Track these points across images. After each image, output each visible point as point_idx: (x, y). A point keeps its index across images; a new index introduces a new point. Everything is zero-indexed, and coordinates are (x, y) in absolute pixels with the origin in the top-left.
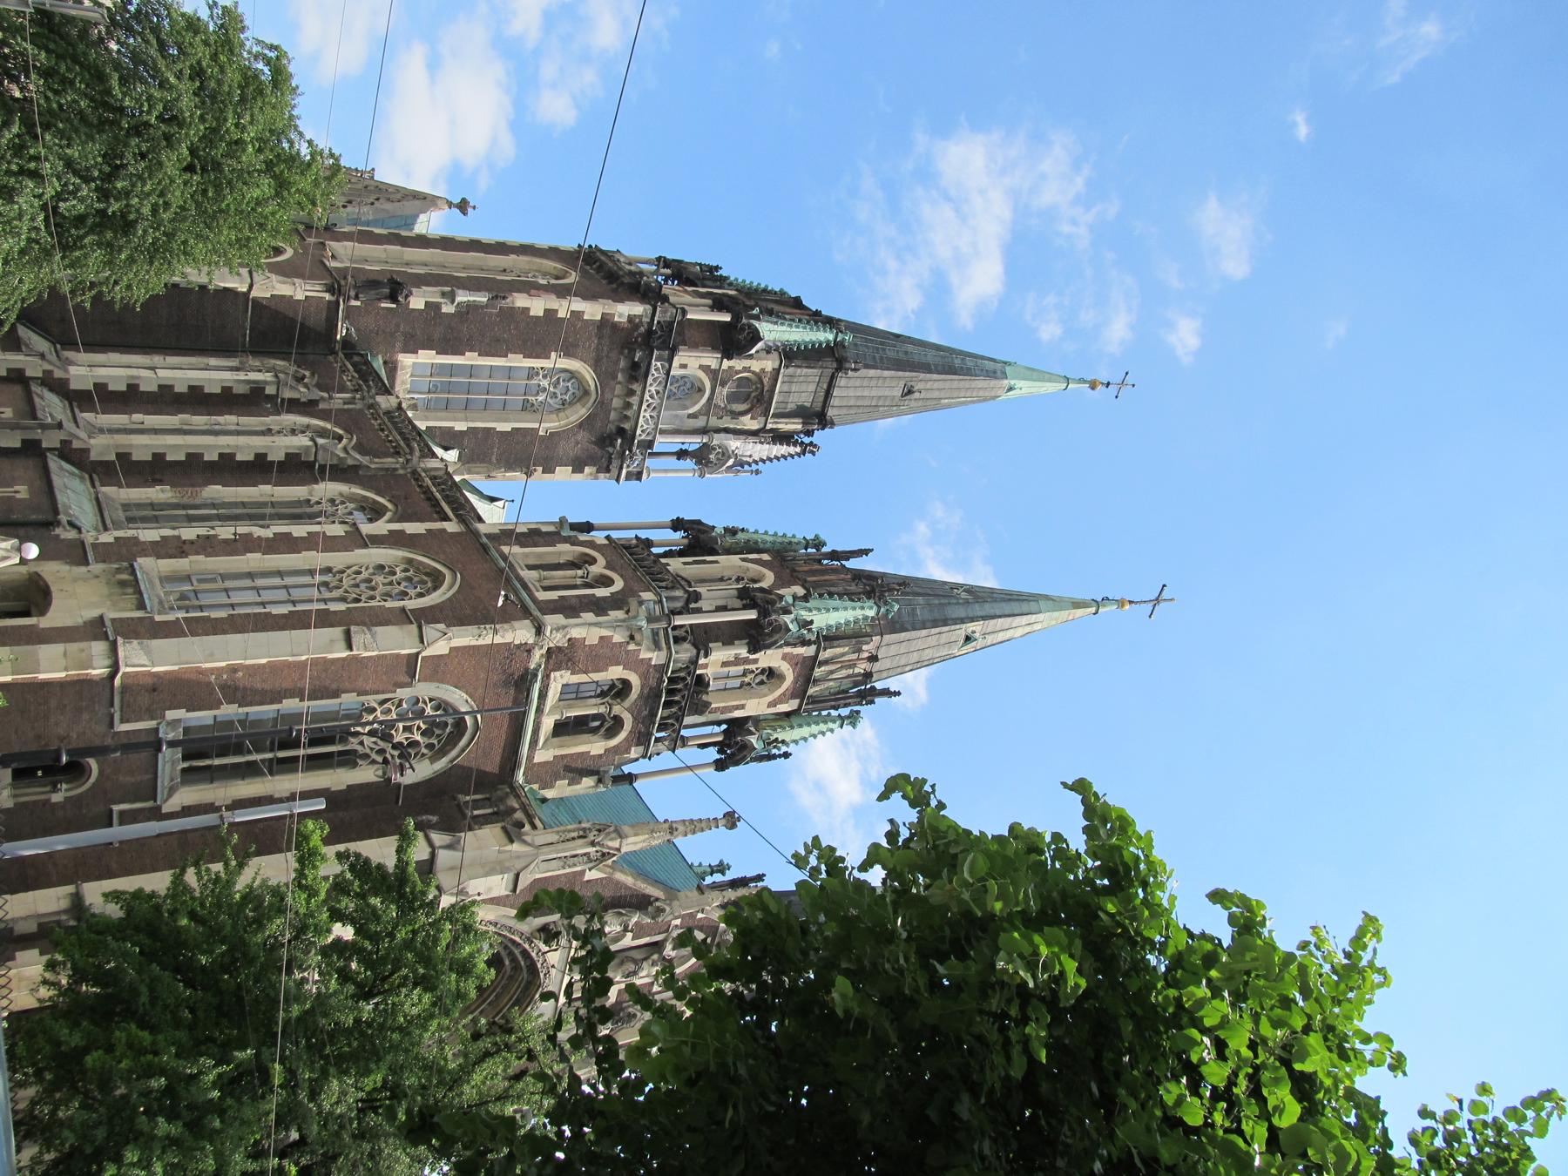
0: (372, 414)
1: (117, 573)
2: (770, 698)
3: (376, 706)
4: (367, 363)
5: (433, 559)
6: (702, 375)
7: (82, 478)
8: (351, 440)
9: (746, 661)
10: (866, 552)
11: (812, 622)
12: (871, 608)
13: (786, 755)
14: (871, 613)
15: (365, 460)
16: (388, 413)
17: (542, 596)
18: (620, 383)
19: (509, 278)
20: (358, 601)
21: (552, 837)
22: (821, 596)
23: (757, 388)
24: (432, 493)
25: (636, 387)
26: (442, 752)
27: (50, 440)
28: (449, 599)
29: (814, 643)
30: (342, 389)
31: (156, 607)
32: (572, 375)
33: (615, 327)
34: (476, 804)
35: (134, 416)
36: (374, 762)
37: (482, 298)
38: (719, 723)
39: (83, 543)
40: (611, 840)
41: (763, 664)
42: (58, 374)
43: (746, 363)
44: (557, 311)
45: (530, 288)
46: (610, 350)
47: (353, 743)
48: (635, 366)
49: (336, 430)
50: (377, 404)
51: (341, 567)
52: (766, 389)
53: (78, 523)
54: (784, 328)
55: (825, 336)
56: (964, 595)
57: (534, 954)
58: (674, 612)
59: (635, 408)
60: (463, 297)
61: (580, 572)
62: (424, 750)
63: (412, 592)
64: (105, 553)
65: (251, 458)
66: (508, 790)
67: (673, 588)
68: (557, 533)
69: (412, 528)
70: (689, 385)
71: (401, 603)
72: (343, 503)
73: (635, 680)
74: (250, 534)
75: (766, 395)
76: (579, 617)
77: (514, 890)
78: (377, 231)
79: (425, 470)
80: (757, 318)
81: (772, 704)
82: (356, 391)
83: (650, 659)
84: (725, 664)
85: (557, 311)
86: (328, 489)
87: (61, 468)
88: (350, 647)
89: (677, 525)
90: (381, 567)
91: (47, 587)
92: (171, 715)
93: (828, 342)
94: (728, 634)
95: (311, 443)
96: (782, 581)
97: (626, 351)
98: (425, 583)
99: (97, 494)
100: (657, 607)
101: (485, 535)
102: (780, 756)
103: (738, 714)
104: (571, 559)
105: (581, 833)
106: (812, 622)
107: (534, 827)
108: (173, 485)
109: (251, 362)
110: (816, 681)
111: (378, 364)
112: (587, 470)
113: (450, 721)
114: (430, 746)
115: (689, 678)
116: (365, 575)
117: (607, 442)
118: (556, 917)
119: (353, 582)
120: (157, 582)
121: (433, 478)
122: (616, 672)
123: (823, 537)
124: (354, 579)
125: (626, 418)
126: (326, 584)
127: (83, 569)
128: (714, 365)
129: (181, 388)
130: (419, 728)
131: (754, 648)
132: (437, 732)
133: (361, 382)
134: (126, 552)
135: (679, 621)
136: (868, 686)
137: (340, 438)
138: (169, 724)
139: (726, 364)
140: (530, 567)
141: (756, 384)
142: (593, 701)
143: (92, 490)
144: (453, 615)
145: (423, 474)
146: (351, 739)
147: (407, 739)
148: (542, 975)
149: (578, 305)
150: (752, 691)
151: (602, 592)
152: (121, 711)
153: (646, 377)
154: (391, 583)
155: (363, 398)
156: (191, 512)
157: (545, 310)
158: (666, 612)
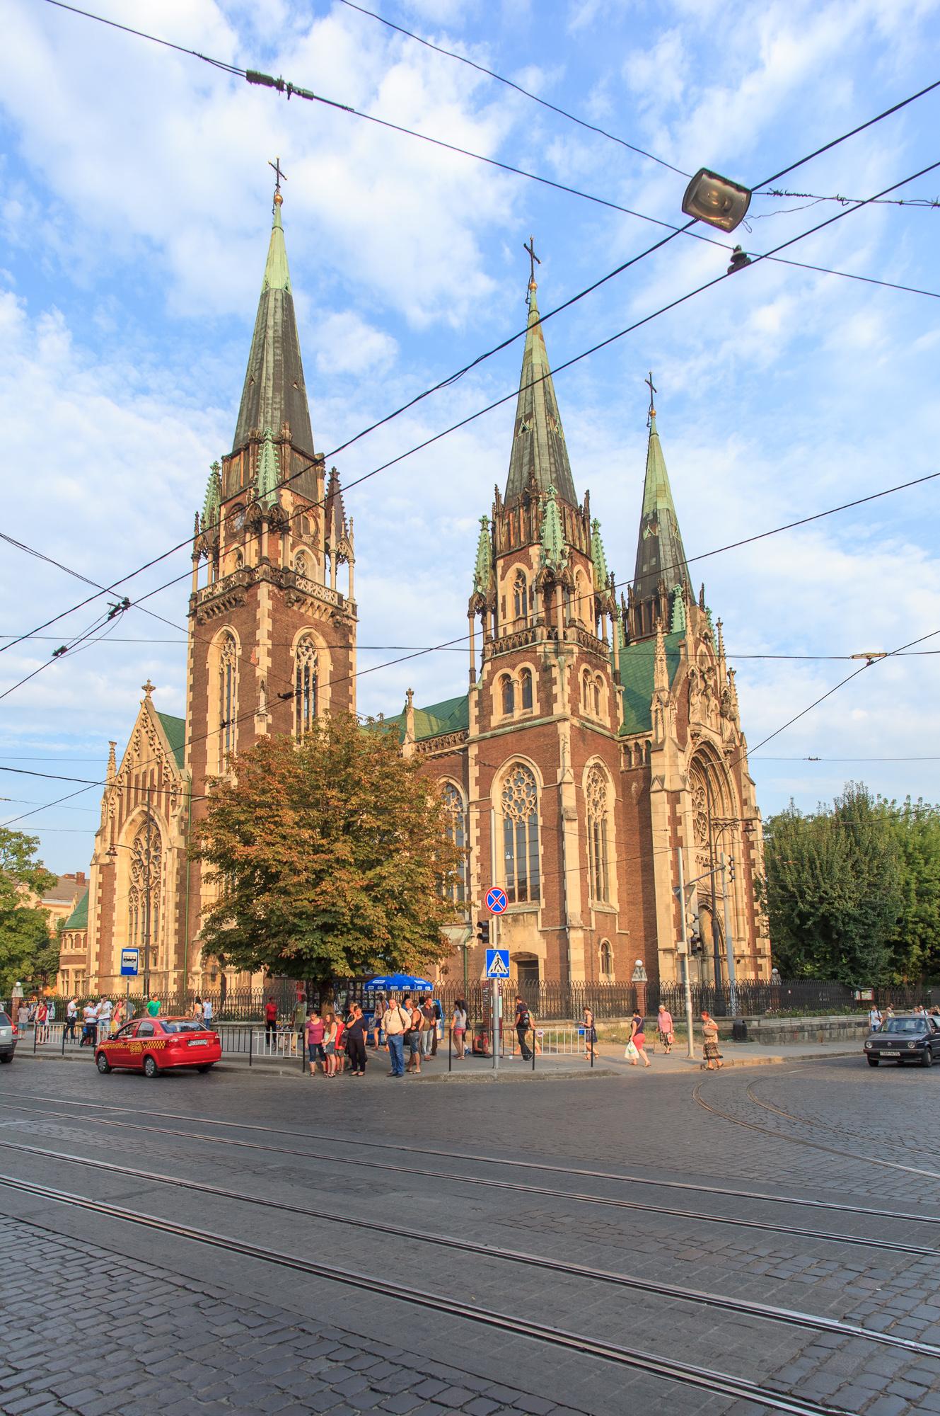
6: (296, 550)
17: (536, 708)
25: (310, 600)
26: (604, 776)
33: (275, 609)
37: (263, 696)
45: (247, 663)
46: (287, 615)
52: (303, 504)
59: (321, 603)
61: (515, 685)
68: (480, 691)
69: (474, 772)
71: (539, 788)
73: (584, 666)
74: (477, 857)
76: (556, 694)
92: (590, 906)
97: (289, 604)
107: (651, 735)
112: (351, 641)
118: (688, 730)
125: (326, 609)
128: (290, 540)
138: (592, 905)
139: (291, 533)
144: (550, 764)
149: (262, 635)
151: (535, 677)
153: (304, 593)
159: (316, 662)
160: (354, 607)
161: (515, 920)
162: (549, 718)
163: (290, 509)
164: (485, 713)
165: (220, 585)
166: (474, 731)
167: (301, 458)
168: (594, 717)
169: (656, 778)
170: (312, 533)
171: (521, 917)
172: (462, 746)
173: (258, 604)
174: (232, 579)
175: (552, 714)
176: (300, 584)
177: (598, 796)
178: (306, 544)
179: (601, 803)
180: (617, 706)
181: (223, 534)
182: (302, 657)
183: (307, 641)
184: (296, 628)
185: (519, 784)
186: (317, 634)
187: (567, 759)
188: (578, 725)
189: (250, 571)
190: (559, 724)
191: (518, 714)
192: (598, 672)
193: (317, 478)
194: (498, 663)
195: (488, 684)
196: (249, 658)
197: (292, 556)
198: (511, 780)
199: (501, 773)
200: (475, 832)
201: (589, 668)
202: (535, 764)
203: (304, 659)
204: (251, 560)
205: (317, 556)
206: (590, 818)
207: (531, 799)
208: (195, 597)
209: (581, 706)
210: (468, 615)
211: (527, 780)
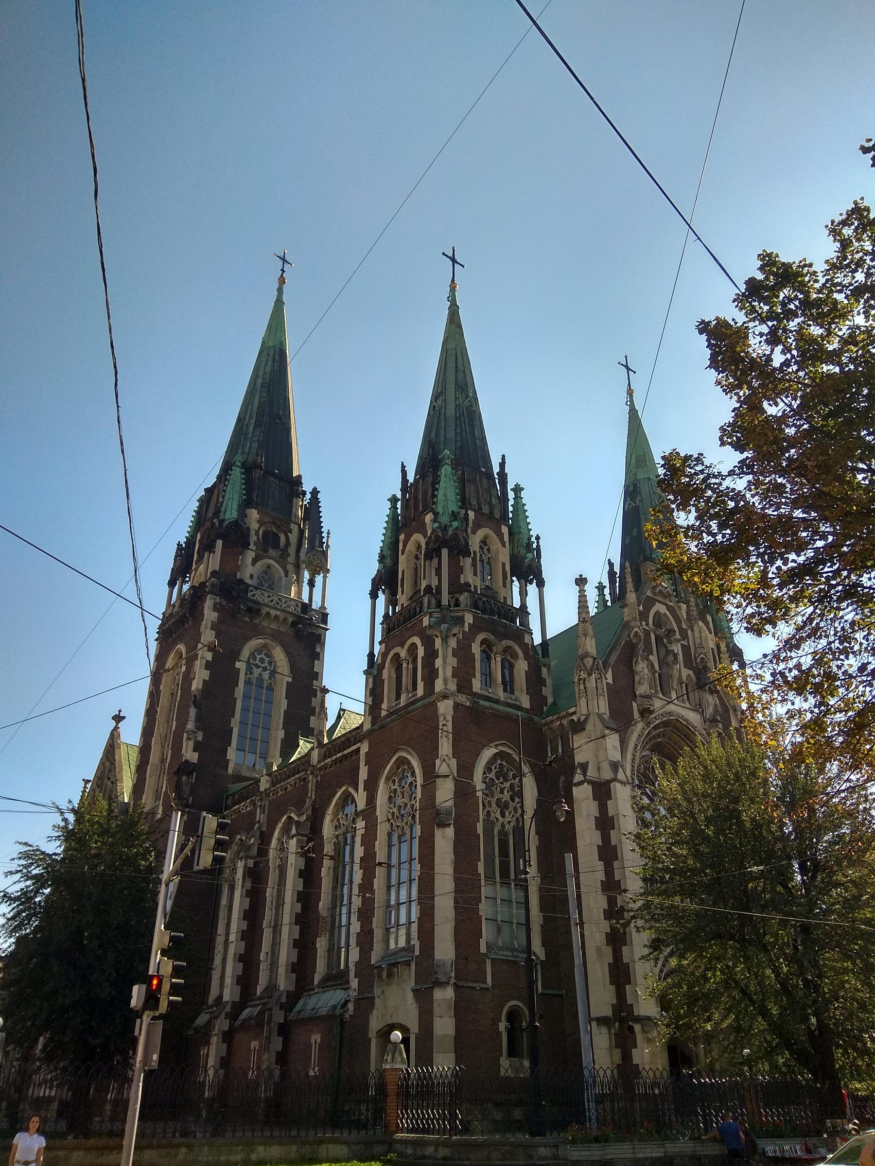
0: (273, 794)
1: (382, 976)
2: (500, 545)
4: (233, 795)
5: (388, 763)
9: (474, 559)
10: (403, 467)
11: (452, 511)
13: (538, 538)
14: (449, 468)
15: (308, 803)
16: (273, 784)
17: (420, 692)
18: (260, 622)
19: (179, 692)
20: (414, 817)
21: (583, 701)
23: (270, 527)
24: (337, 759)
27: (279, 1016)
28: (418, 755)
29: (467, 511)
30: (252, 814)
31: (410, 954)
32: (252, 655)
34: (554, 750)
35: (261, 959)
37: (193, 711)
38: (512, 581)
40: (588, 663)
41: (477, 549)
42: (228, 1009)
43: (252, 533)
44: (207, 661)
45: (188, 678)
47: (509, 828)
48: (249, 610)
49: (283, 821)
50: (265, 790)
51: (388, 826)
52: (271, 520)
53: (343, 1001)
55: (237, 473)
56: (439, 402)
57: (657, 722)
58: (439, 605)
59: (278, 613)
60: (190, 726)
61: (404, 665)
63: (410, 779)
64: (366, 985)
65: (301, 881)
66: (547, 727)
67: (422, 603)
68: (375, 678)
69: (363, 773)
70: (264, 575)
71: (419, 787)
74: (360, 886)
77: (616, 731)
79: (319, 762)
80: (222, 522)
81: (504, 545)
82: (254, 804)
83: (469, 624)
84: (475, 574)
85: (207, 661)
86: (328, 829)
87: (299, 1012)
89: (374, 595)
90: (390, 797)
91: (388, 1025)
92: (483, 949)
94: (456, 570)
95: (295, 839)
96: (422, 529)
97: (239, 615)
98: (404, 770)
99: (318, 986)
101: (372, 726)
102: (538, 542)
103: (508, 569)
104: (394, 670)
105: (582, 682)
106: (452, 511)
107: (575, 713)
108: (317, 935)
109: (226, 876)
110: (491, 513)
111: (235, 787)
112: (318, 650)
113: (499, 762)
114: (514, 777)
115: (484, 599)
116: (395, 810)
121: (325, 758)
122: (476, 649)
125: (285, 619)
126: (399, 837)
127: (377, 1001)
129: (244, 925)
133: (249, 801)
135: (445, 601)
136: (496, 476)
137: (290, 818)
139: (252, 547)
140: (398, 697)
142: (493, 665)
143: (316, 991)
145: (322, 763)
147: (508, 792)
148: (671, 718)
150: (493, 556)
151: (421, 652)
152: (478, 982)
153: (258, 603)
154: (403, 793)
155: (261, 800)
156: (337, 925)
158: (439, 610)
160: (324, 617)
161: (390, 975)
163: (255, 526)
165: (177, 605)
170: (281, 548)
176: (254, 596)
177: (506, 796)
178: (271, 558)
179: (512, 805)
180: (543, 682)
181: (195, 558)
184: (248, 639)
186: (273, 644)
187: (445, 747)
188: (468, 704)
192: (510, 643)
196: (190, 672)
199: (386, 771)
200: (359, 852)
201: (492, 637)
202: (413, 753)
203: (257, 672)
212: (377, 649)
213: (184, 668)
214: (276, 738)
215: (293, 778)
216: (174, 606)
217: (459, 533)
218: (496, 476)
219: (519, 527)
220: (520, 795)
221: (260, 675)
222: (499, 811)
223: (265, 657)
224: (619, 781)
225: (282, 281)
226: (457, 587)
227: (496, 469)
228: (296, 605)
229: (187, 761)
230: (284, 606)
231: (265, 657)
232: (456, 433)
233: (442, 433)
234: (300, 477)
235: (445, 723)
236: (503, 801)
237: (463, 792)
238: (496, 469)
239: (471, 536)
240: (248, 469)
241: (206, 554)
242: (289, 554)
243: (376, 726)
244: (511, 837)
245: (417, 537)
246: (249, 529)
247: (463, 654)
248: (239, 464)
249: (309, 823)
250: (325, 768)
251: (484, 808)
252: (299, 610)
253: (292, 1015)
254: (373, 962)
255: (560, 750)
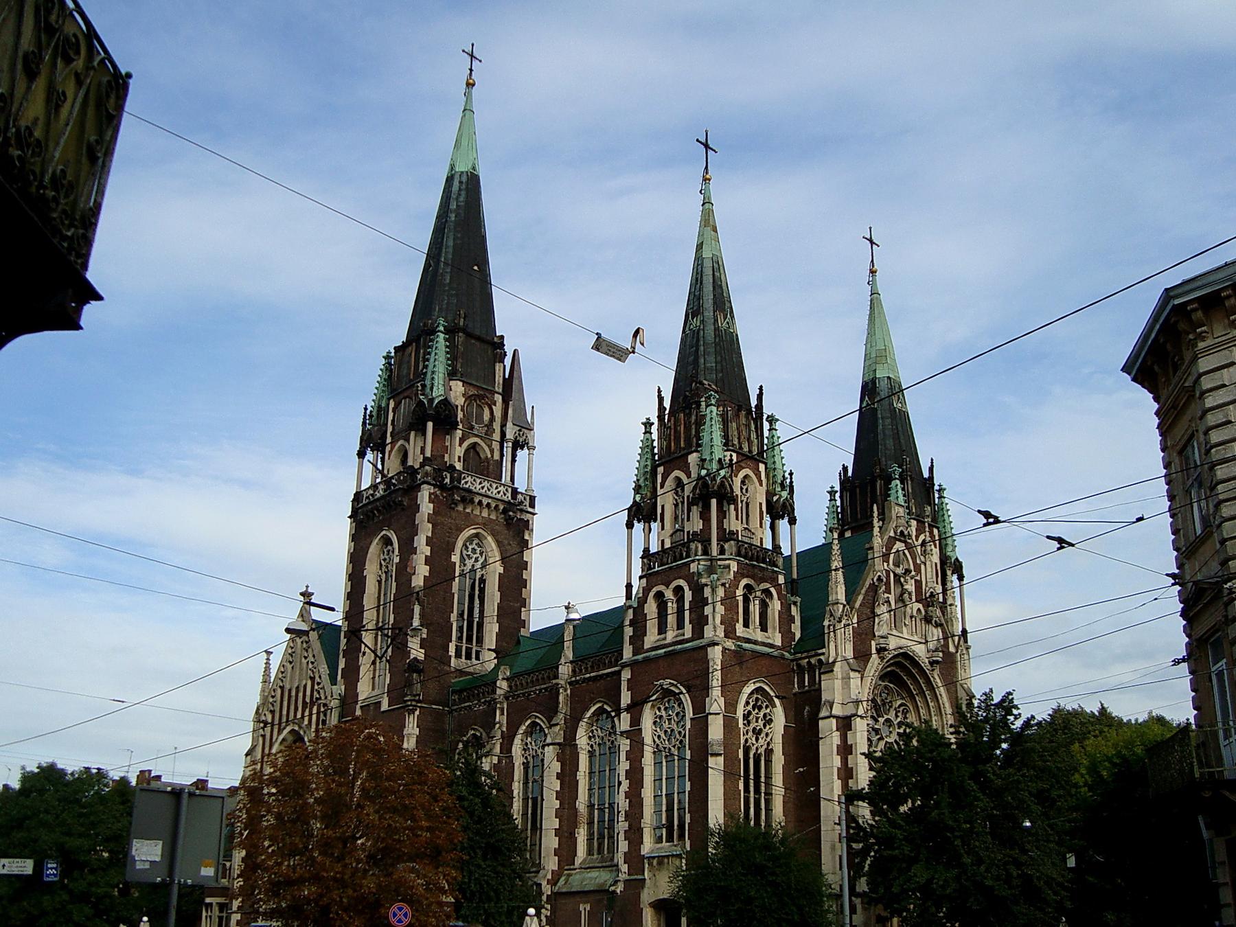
1: (652, 865)
3: (745, 737)
6: (466, 444)
7: (569, 875)
8: (536, 717)
10: (659, 391)
11: (720, 459)
12: (711, 411)
13: (791, 474)
14: (714, 409)
17: (688, 631)
20: (681, 742)
22: (699, 445)
24: (590, 677)
25: (477, 500)
29: (731, 456)
32: (465, 545)
36: (771, 740)
37: (417, 609)
39: (627, 880)
44: (426, 556)
45: (404, 572)
48: (463, 500)
49: (527, 724)
54: (436, 377)
59: (490, 501)
60: (416, 622)
62: (768, 711)
67: (688, 548)
68: (634, 608)
69: (626, 698)
72: (592, 731)
73: (744, 582)
75: (482, 393)
77: (859, 672)
78: (342, 664)
80: (431, 401)
81: (761, 485)
84: (737, 519)
85: (426, 556)
88: (720, 755)
89: (630, 525)
90: (655, 723)
93: (446, 340)
94: (722, 514)
95: (551, 747)
97: (453, 506)
98: (669, 700)
100: (702, 563)
101: (633, 656)
102: (791, 478)
105: (831, 627)
110: (750, 451)
113: (755, 696)
114: (767, 707)
117: (510, 521)
119: (667, 742)
120: (660, 845)
122: (740, 592)
123: (645, 420)
124: (664, 740)
125: (497, 506)
127: (648, 881)
128: (459, 433)
130: (757, 714)
131: (733, 500)
132: (759, 703)
134: (635, 859)
135: (715, 551)
136: (754, 410)
139: (460, 427)
140: (662, 629)
141: (471, 401)
142: (751, 607)
144: (700, 691)
145: (573, 679)
146: (759, 752)
149: (421, 542)
151: (688, 595)
155: (501, 703)
157: (426, 564)
159: (484, 566)
161: (660, 863)
162: (701, 640)
163: (460, 401)
164: (639, 633)
166: (627, 653)
167: (478, 343)
168: (759, 636)
169: (826, 701)
171: (666, 860)
172: (616, 669)
173: (417, 508)
174: (394, 481)
175: (703, 637)
176: (466, 483)
177: (761, 723)
178: (477, 436)
180: (792, 620)
181: (390, 429)
182: (467, 561)
183: (475, 542)
185: (670, 713)
186: (485, 534)
188: (733, 648)
189: (412, 472)
190: (709, 649)
191: (670, 636)
193: (495, 362)
194: (654, 579)
195: (642, 601)
197: (459, 451)
198: (662, 708)
200: (624, 766)
203: (469, 563)
204: (414, 460)
205: (489, 446)
206: (747, 751)
207: (681, 730)
208: (358, 496)
209: (739, 627)
210: (627, 525)
211: (677, 709)
212: (636, 584)
213: (397, 560)
214: (491, 631)
215: (538, 688)
216: (374, 487)
217: (726, 479)
218: (754, 410)
219: (774, 462)
220: (771, 721)
221: (473, 566)
222: (754, 739)
223: (476, 547)
224: (858, 716)
225: (470, 85)
226: (725, 536)
227: (754, 402)
228: (507, 490)
229: (415, 659)
230: (495, 491)
231: (476, 547)
232: (716, 362)
233: (702, 361)
234: (502, 337)
235: (715, 667)
236: (758, 728)
237: (730, 725)
238: (754, 402)
239: (734, 478)
240: (451, 331)
241: (413, 434)
242: (494, 430)
243: (640, 657)
244: (763, 758)
245: (677, 473)
246: (457, 406)
247: (729, 601)
248: (442, 328)
249: (562, 732)
250: (577, 682)
251: (744, 735)
252: (509, 495)
253: (556, 889)
254: (642, 853)
255: (806, 684)
